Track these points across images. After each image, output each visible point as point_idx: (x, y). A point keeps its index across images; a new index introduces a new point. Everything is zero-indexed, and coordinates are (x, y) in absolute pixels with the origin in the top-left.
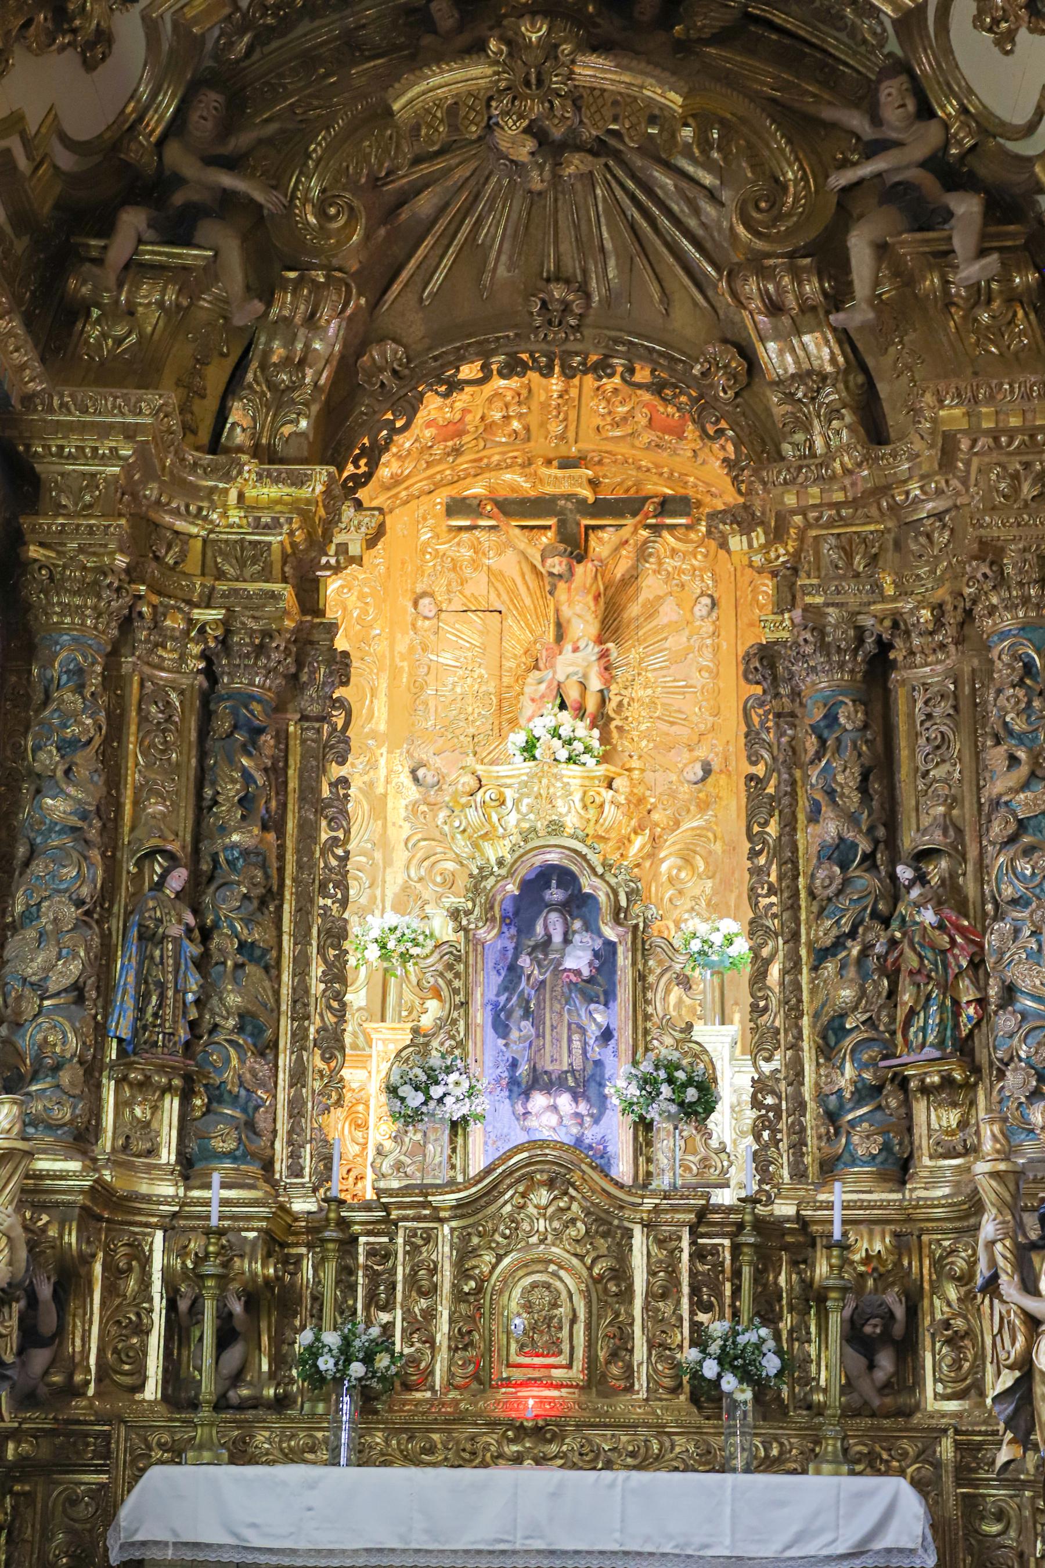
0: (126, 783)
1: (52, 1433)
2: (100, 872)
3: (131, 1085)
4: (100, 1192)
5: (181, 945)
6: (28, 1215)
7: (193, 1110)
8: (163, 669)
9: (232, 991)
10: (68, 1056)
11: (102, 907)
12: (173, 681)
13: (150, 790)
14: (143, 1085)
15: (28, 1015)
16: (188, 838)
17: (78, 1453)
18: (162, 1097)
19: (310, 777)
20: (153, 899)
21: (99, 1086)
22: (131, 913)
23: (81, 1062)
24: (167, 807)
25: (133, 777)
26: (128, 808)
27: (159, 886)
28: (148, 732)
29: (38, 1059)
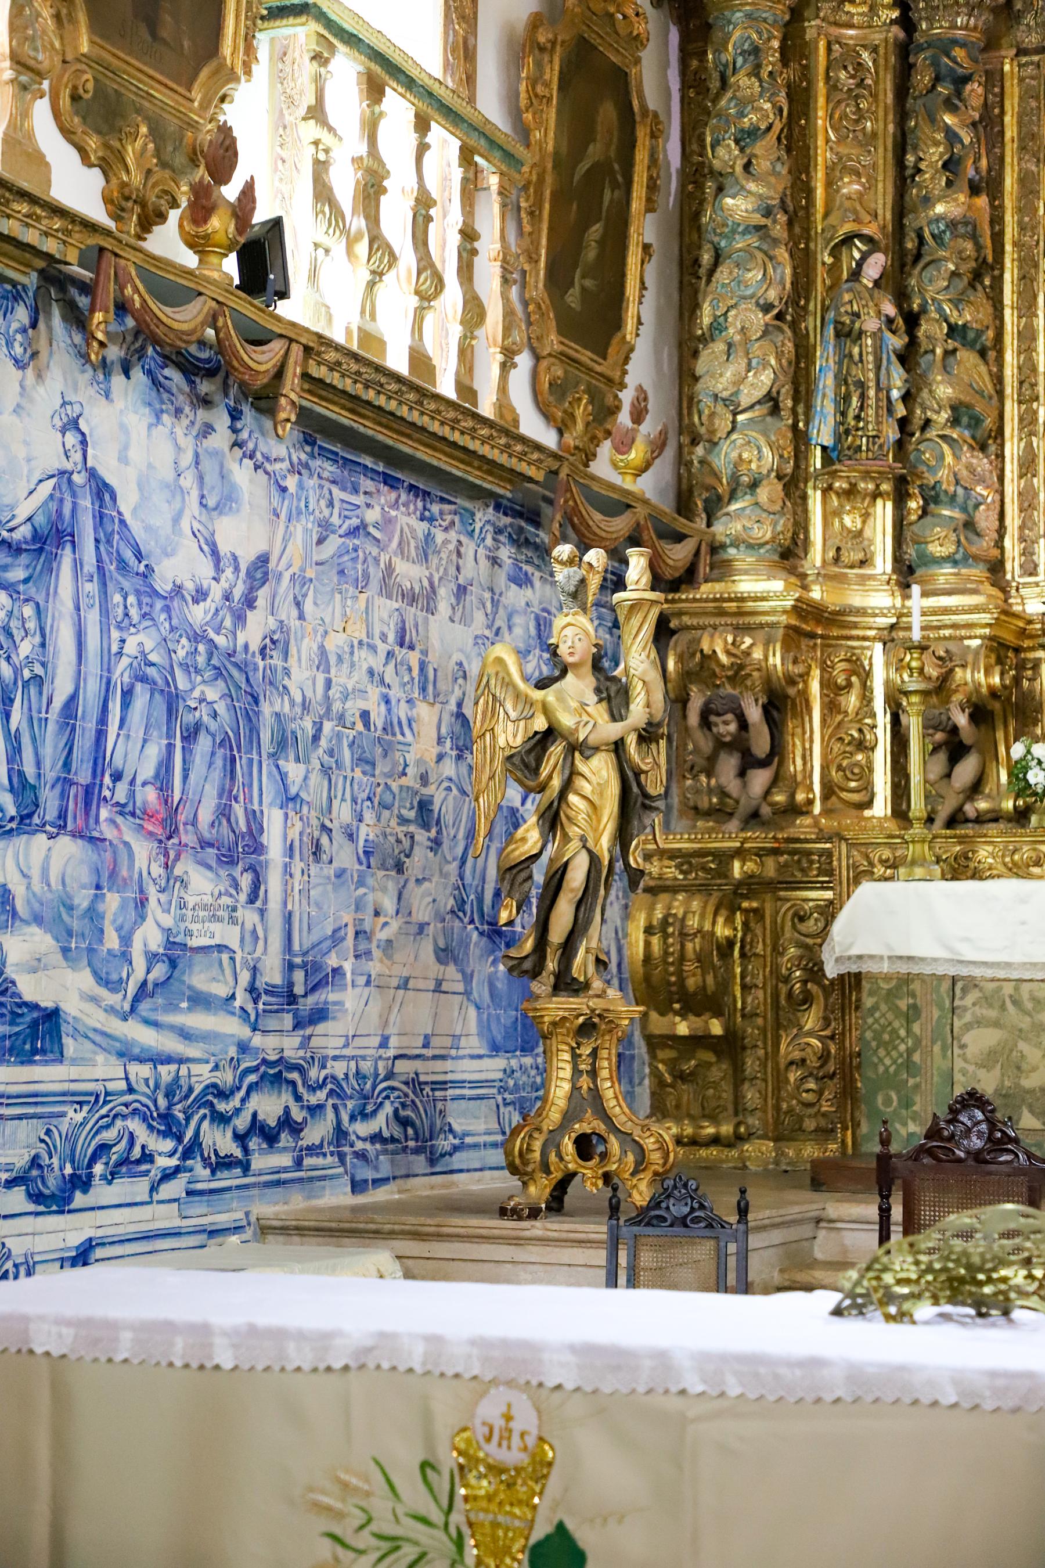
0: (816, 165)
5: (881, 339)
6: (730, 639)
7: (909, 513)
8: (851, 26)
9: (941, 382)
10: (765, 472)
12: (865, 38)
13: (844, 167)
14: (851, 492)
15: (721, 433)
16: (889, 216)
19: (1031, 122)
20: (848, 291)
21: (804, 497)
23: (779, 477)
24: (863, 185)
25: (823, 156)
26: (820, 193)
27: (856, 275)
28: (839, 102)
29: (735, 478)
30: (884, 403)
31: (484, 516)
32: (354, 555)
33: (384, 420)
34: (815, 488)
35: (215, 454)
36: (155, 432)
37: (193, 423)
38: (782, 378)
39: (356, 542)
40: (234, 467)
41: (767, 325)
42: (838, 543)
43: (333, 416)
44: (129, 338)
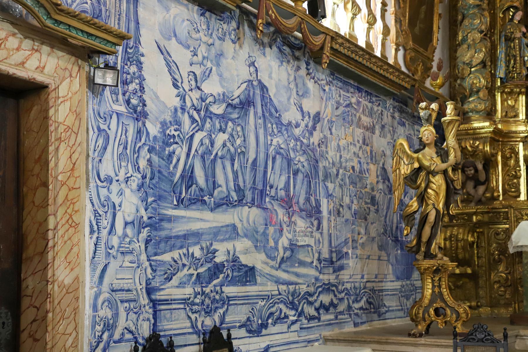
1: (488, 213)
2: (488, 19)
3: (506, 93)
4: (497, 132)
6: (471, 142)
10: (482, 87)
11: (491, 32)
15: (466, 75)
17: (497, 218)
18: (518, 96)
22: (502, 32)
23: (487, 88)
27: (512, 20)
29: (471, 90)
30: (523, 61)
31: (390, 102)
32: (348, 113)
33: (358, 66)
34: (498, 92)
35: (301, 77)
36: (280, 68)
37: (293, 66)
38: (487, 55)
39: (349, 109)
40: (308, 82)
41: (481, 38)
42: (506, 110)
43: (341, 64)
44: (271, 35)
